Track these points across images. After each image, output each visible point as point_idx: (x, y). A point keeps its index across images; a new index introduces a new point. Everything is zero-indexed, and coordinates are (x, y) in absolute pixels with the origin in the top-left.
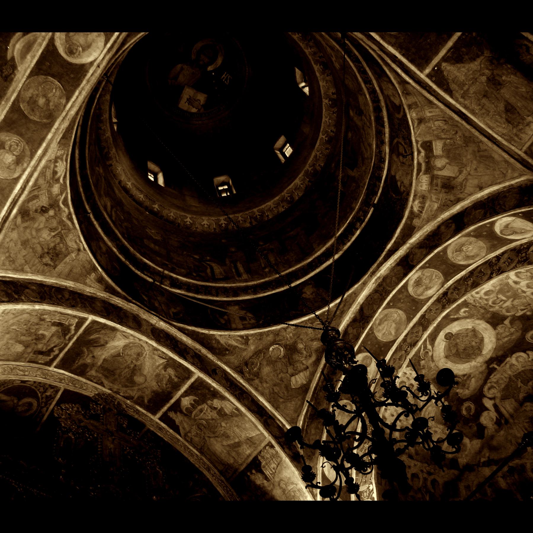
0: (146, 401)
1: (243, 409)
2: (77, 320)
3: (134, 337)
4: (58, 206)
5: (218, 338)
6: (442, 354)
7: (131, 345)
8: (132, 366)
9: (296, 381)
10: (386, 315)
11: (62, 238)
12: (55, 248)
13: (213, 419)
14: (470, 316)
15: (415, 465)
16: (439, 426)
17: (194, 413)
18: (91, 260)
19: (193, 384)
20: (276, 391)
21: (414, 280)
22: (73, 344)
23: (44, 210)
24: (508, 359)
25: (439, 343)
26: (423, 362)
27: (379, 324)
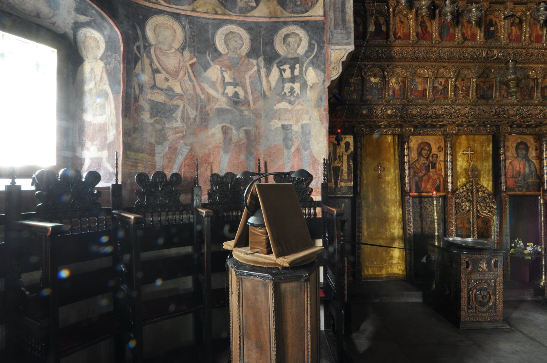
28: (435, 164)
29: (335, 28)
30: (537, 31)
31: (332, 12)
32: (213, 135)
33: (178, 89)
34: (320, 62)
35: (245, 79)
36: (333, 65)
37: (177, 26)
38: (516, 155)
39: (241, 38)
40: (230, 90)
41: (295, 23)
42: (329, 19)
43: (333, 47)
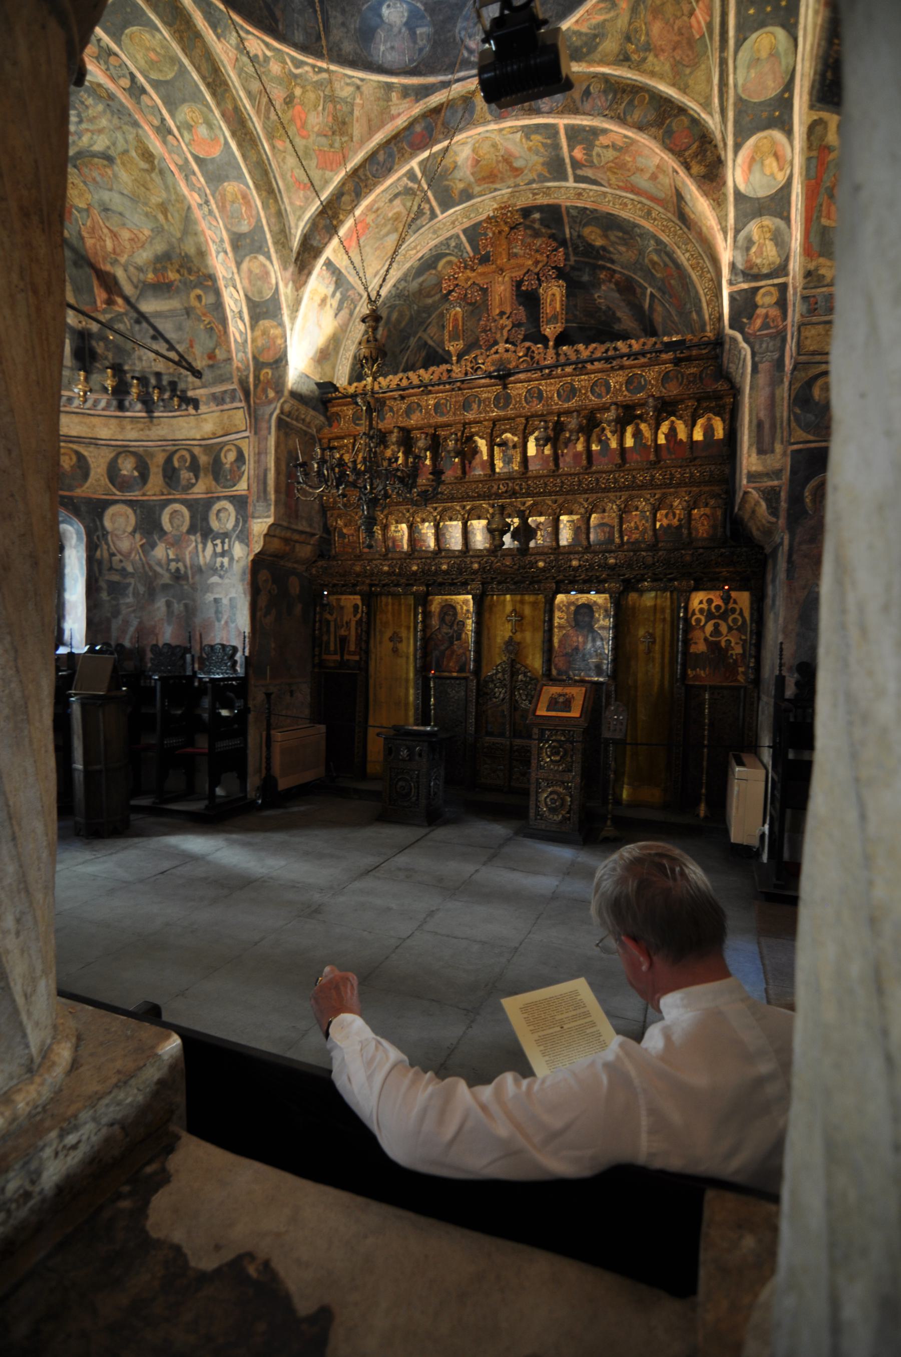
0: (547, 175)
1: (629, 134)
2: (405, 179)
3: (471, 137)
4: (296, 76)
5: (576, 28)
7: (477, 145)
8: (500, 158)
9: (699, 22)
11: (332, 99)
12: (335, 118)
13: (616, 158)
17: (595, 161)
18: (379, 82)
19: (566, 134)
20: (678, 58)
23: (289, 101)
28: (460, 634)
29: (258, 501)
30: (575, 448)
31: (255, 484)
32: (159, 608)
33: (130, 569)
34: (244, 537)
35: (185, 554)
36: (255, 539)
37: (129, 511)
38: (573, 624)
39: (183, 516)
40: (173, 566)
41: (226, 498)
42: (252, 491)
43: (255, 521)
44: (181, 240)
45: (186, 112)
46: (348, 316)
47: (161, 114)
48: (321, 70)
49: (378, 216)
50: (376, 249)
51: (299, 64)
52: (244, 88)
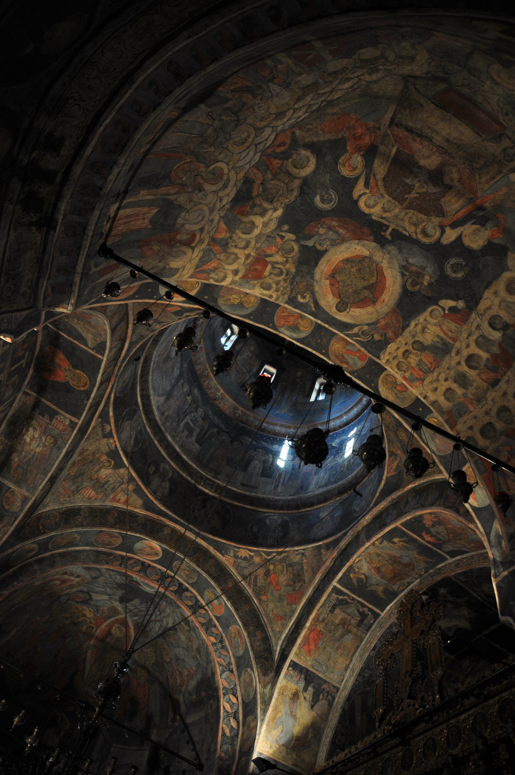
3: (360, 555)
5: (389, 475)
6: (370, 309)
7: (368, 559)
10: (337, 356)
11: (291, 565)
12: (294, 575)
14: (310, 289)
15: (508, 382)
16: (471, 320)
21: (291, 334)
22: (359, 597)
23: (267, 573)
24: (374, 218)
25: (353, 317)
26: (377, 337)
27: (347, 363)
44: (206, 668)
45: (208, 595)
46: (326, 706)
47: (196, 598)
48: (281, 553)
49: (326, 624)
50: (337, 649)
51: (268, 554)
52: (240, 574)
